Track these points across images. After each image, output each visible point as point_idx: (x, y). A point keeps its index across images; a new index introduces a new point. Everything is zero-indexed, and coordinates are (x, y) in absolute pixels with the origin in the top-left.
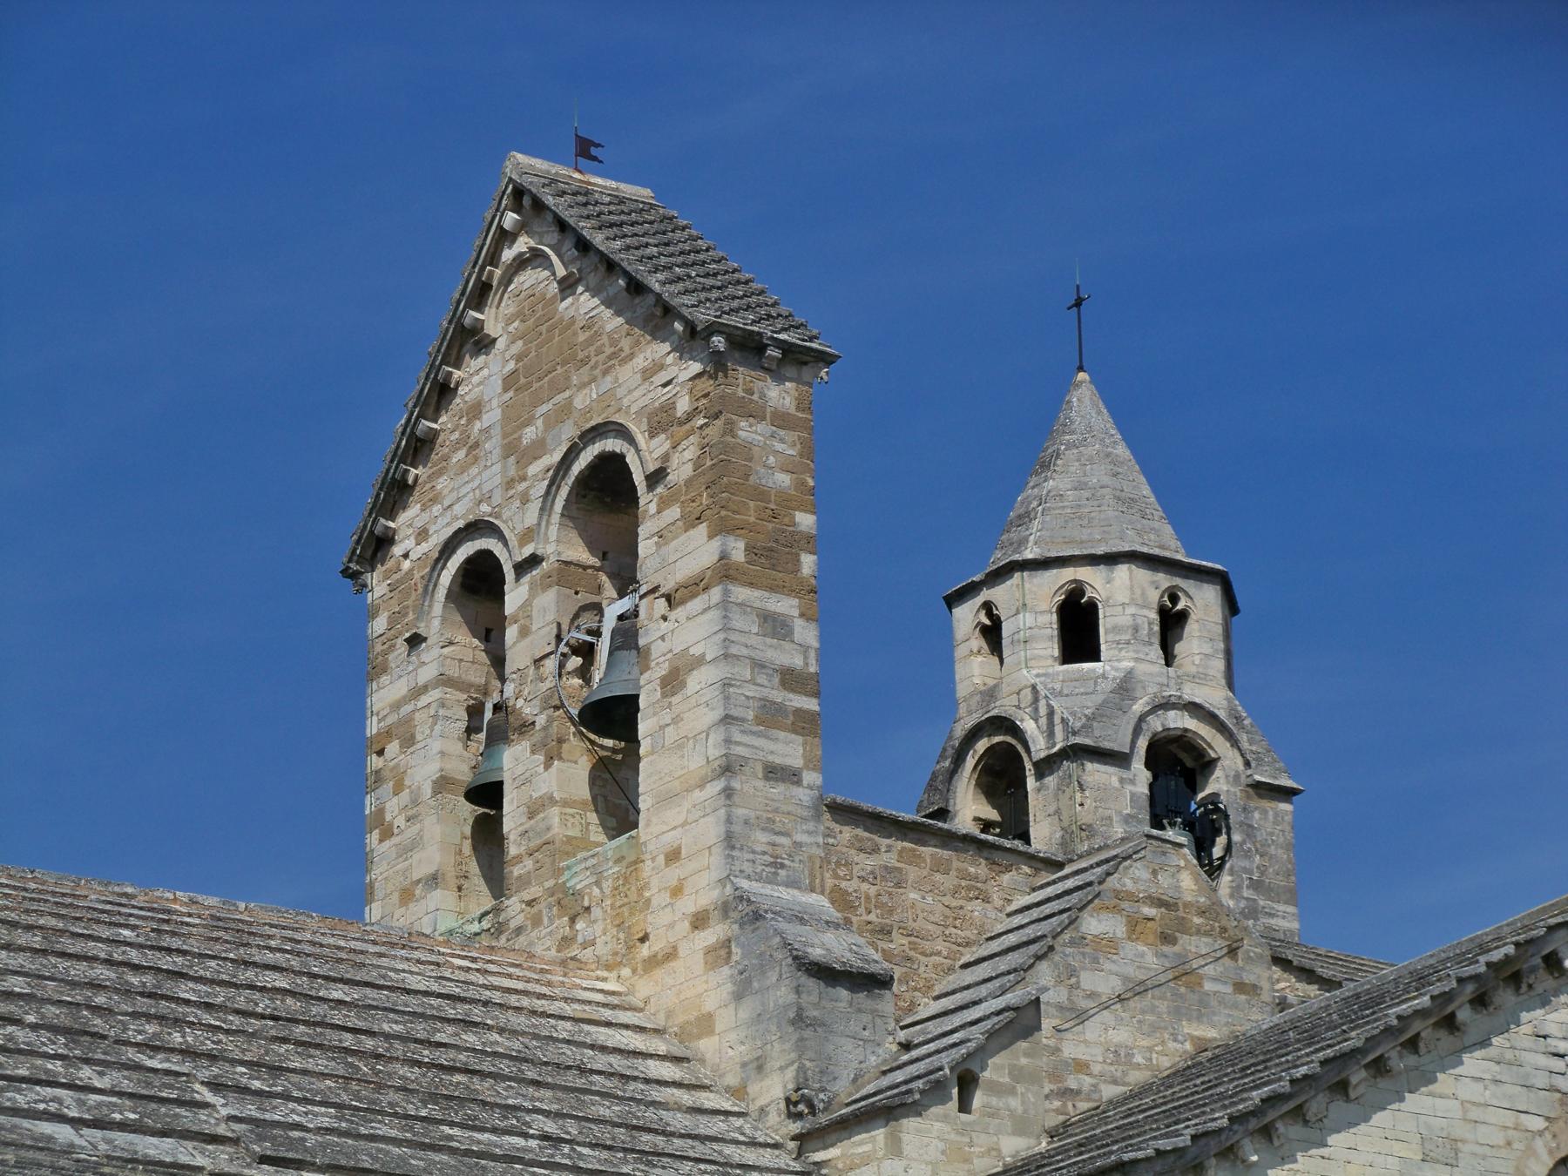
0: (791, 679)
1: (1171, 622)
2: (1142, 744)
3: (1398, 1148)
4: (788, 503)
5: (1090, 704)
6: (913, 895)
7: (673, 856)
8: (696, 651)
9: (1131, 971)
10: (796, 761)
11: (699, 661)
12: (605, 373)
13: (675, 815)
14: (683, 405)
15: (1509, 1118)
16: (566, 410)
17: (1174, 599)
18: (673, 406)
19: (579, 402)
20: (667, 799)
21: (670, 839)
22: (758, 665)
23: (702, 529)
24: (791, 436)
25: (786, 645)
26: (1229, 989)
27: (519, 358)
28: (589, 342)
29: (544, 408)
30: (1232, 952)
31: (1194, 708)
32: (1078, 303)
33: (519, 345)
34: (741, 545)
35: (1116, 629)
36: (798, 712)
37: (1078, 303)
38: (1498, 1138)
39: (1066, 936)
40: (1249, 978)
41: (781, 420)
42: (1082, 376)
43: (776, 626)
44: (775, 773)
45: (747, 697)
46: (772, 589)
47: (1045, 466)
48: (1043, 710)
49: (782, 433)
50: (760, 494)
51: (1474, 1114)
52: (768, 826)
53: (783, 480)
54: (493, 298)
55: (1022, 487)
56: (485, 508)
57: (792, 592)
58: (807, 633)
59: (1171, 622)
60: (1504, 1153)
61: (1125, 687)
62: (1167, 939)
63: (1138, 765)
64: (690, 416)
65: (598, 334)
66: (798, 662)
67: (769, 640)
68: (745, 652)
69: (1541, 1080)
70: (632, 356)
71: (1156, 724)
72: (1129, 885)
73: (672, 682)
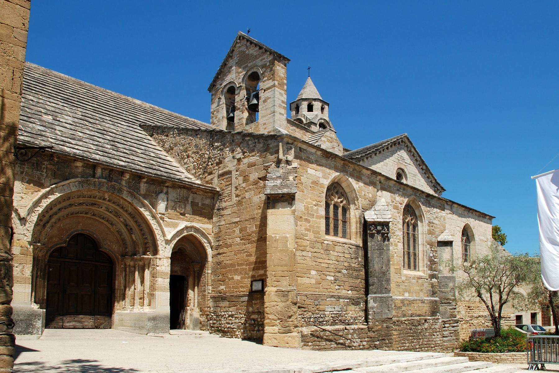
0: (283, 102)
1: (322, 109)
2: (319, 123)
4: (283, 79)
5: (313, 117)
6: (297, 133)
7: (265, 124)
8: (269, 97)
9: (327, 146)
10: (283, 113)
11: (270, 98)
12: (254, 61)
13: (265, 119)
14: (268, 64)
16: (247, 66)
17: (323, 106)
18: (266, 64)
19: (249, 65)
20: (263, 117)
21: (264, 122)
22: (279, 99)
23: (271, 80)
24: (284, 70)
26: (338, 150)
27: (238, 60)
28: (251, 56)
29: (243, 66)
30: (339, 146)
31: (324, 120)
32: (309, 69)
33: (239, 58)
34: (277, 83)
35: (316, 108)
36: (283, 106)
37: (309, 69)
39: (320, 140)
40: (340, 149)
42: (309, 78)
44: (280, 113)
47: (304, 88)
48: (305, 117)
50: (280, 76)
52: (280, 120)
54: (234, 52)
55: (301, 91)
56: (232, 80)
58: (285, 96)
59: (322, 109)
61: (317, 115)
62: (331, 143)
63: (318, 125)
64: (269, 65)
65: (253, 56)
66: (284, 100)
70: (259, 58)
71: (320, 121)
72: (327, 135)
73: (265, 101)
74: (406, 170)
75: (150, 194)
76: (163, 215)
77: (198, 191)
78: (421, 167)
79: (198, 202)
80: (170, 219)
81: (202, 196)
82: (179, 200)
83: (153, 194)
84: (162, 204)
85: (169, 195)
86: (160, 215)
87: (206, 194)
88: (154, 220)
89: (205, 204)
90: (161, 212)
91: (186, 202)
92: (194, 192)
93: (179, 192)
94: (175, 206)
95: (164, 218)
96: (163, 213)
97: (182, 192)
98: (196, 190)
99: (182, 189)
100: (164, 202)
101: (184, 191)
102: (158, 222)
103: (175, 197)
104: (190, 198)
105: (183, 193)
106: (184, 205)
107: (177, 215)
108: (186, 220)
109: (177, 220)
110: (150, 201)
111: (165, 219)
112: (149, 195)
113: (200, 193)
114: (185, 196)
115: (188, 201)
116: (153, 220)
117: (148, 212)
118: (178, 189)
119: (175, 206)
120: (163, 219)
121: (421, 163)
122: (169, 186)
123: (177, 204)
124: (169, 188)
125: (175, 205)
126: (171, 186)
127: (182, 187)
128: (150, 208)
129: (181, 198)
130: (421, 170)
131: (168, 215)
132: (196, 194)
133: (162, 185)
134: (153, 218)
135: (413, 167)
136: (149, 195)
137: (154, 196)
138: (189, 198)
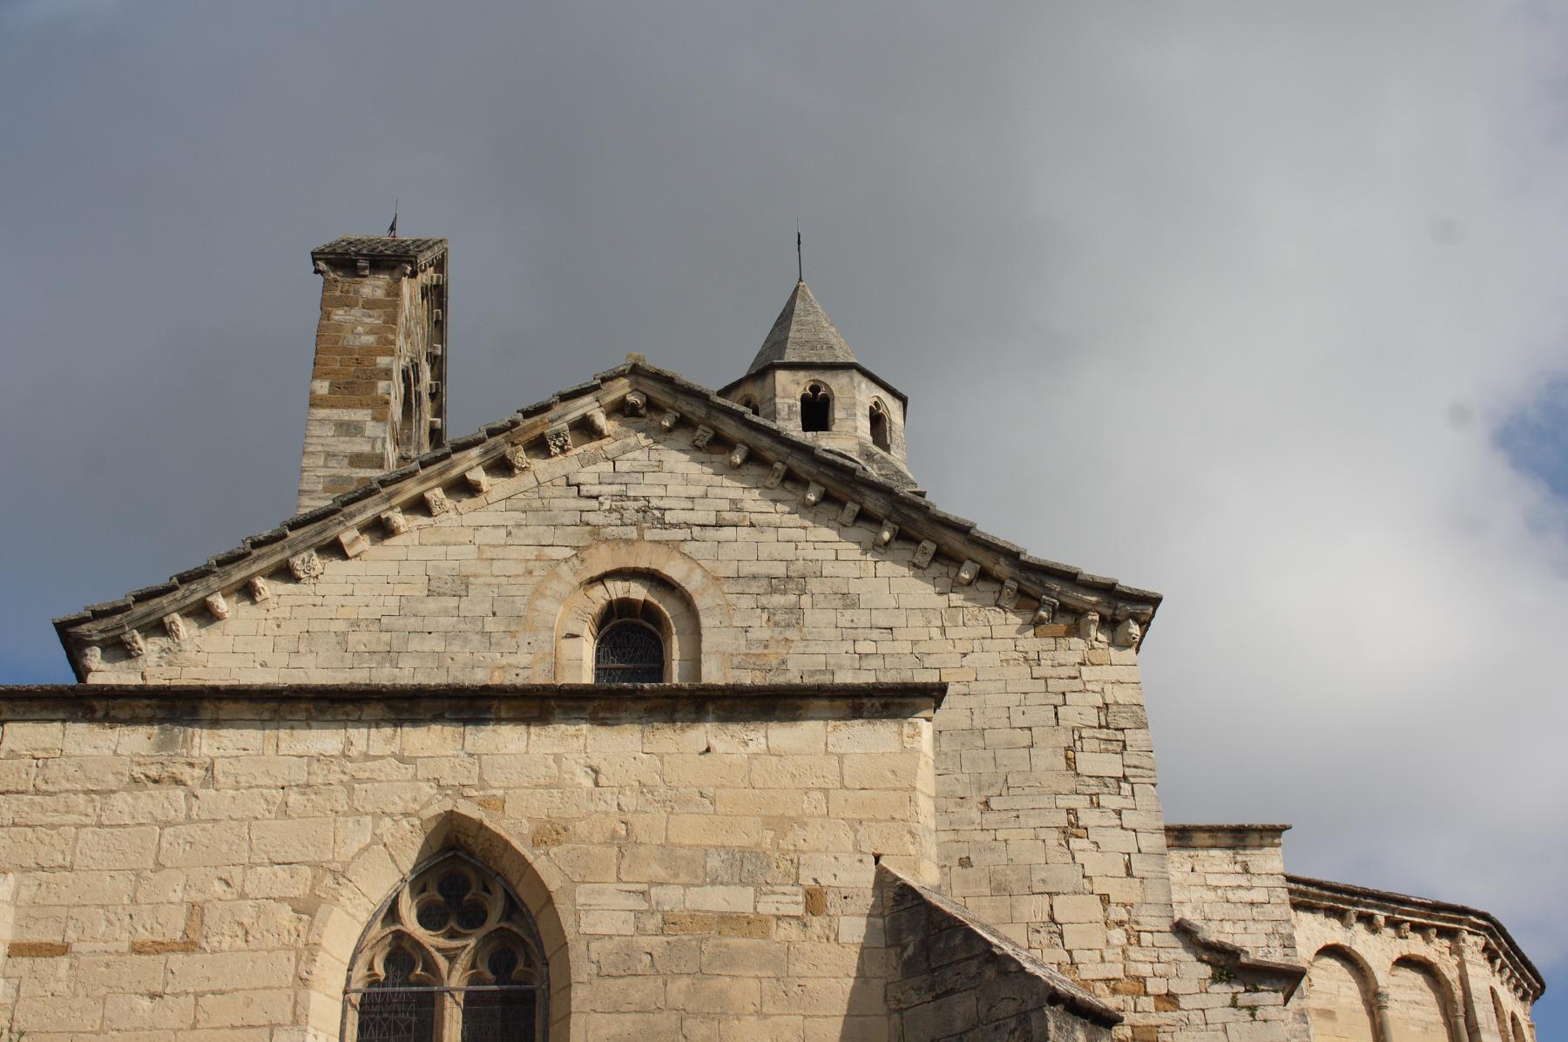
3: (400, 590)
15: (531, 553)
22: (330, 455)
24: (375, 313)
25: (358, 439)
38: (520, 569)
41: (370, 304)
43: (349, 429)
45: (318, 477)
46: (348, 407)
49: (371, 312)
50: (348, 351)
51: (489, 554)
53: (369, 339)
57: (362, 406)
60: (521, 580)
67: (341, 439)
68: (319, 448)
69: (569, 518)
74: (674, 569)
78: (852, 508)
121: (838, 490)
130: (864, 532)
135: (770, 535)
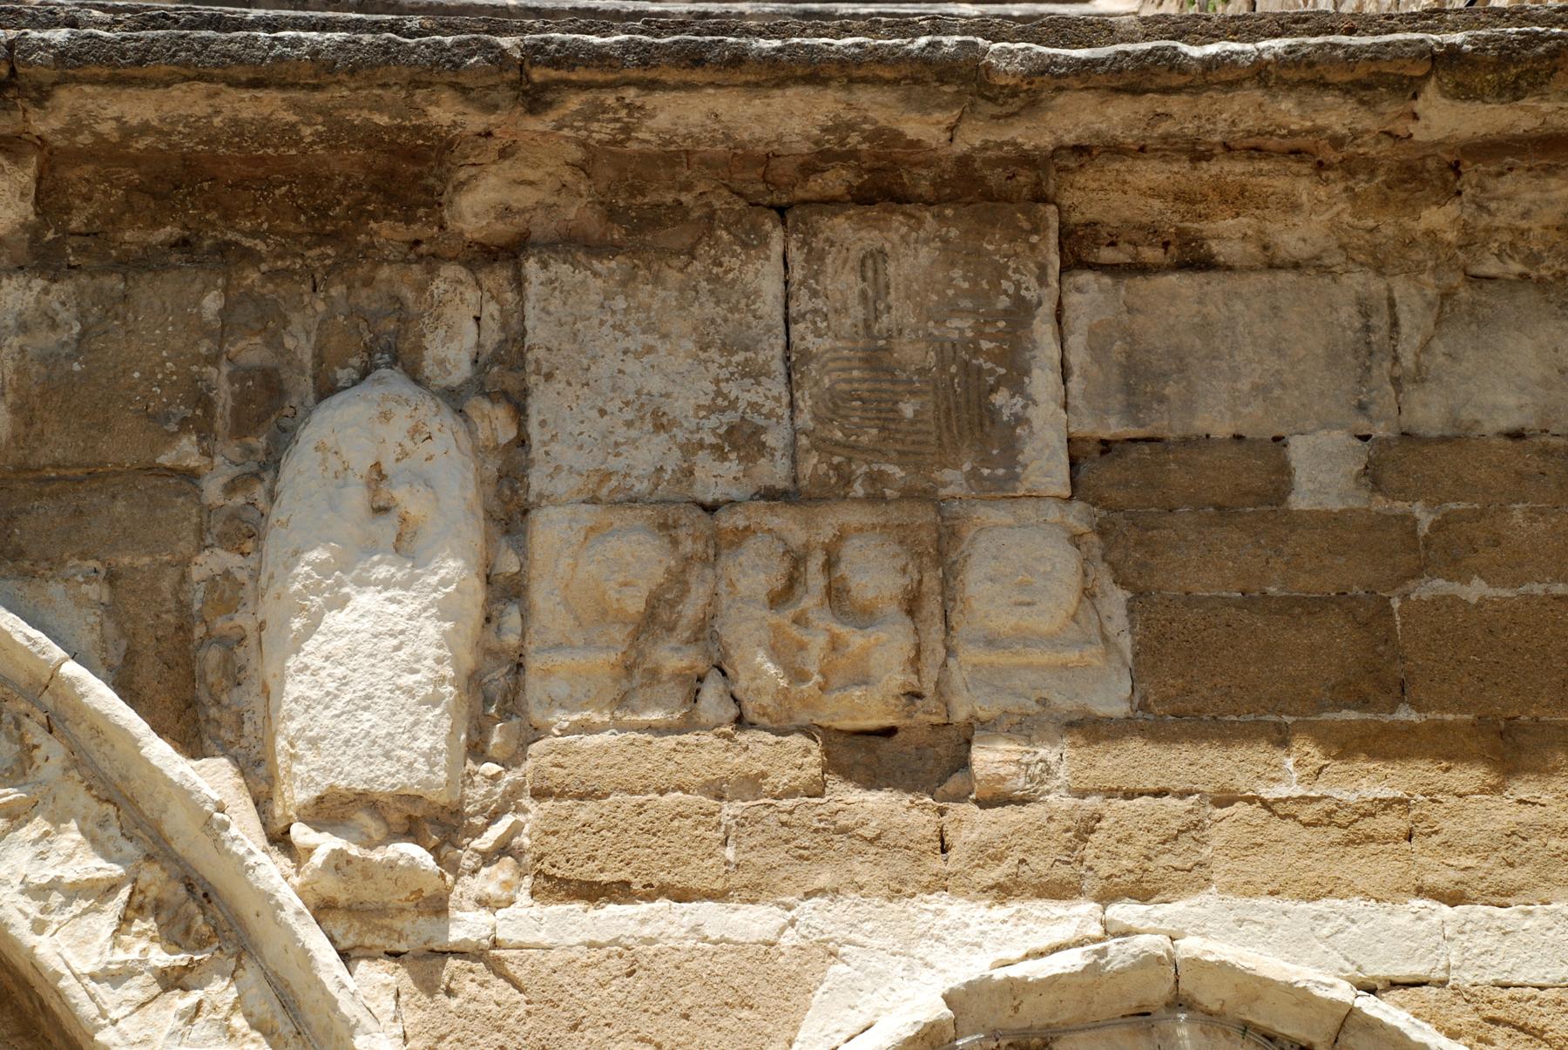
75: (119, 449)
76: (411, 832)
77: (1237, 199)
79: (1256, 420)
80: (593, 892)
81: (1358, 281)
82: (775, 472)
83: (185, 452)
84: (367, 600)
85: (542, 403)
86: (325, 844)
87: (1437, 218)
88: (220, 991)
89: (1456, 439)
90: (354, 774)
91: (953, 480)
92: (1151, 232)
93: (770, 306)
94: (691, 609)
95: (438, 907)
96: (386, 777)
97: (842, 282)
98: (1152, 173)
99: (840, 227)
100: (406, 545)
101: (874, 259)
102: (287, 1000)
103: (682, 406)
104: (1043, 381)
105: (873, 301)
106: (903, 535)
107: (752, 784)
108: (988, 854)
109: (754, 893)
110: (110, 609)
111: (466, 926)
112: (95, 475)
113: (1292, 239)
114: (912, 353)
115: (1011, 448)
116: (172, 981)
117: (71, 836)
118: (753, 242)
119: (691, 609)
120: (415, 931)
122: (542, 226)
123: (721, 545)
124: (531, 266)
125: (678, 581)
126: (576, 211)
127: (835, 181)
128: (101, 728)
129: (833, 407)
131: (535, 812)
132: (1196, 260)
133: (388, 232)
134: (176, 934)
136: (95, 475)
137: (212, 490)
138: (1016, 378)
